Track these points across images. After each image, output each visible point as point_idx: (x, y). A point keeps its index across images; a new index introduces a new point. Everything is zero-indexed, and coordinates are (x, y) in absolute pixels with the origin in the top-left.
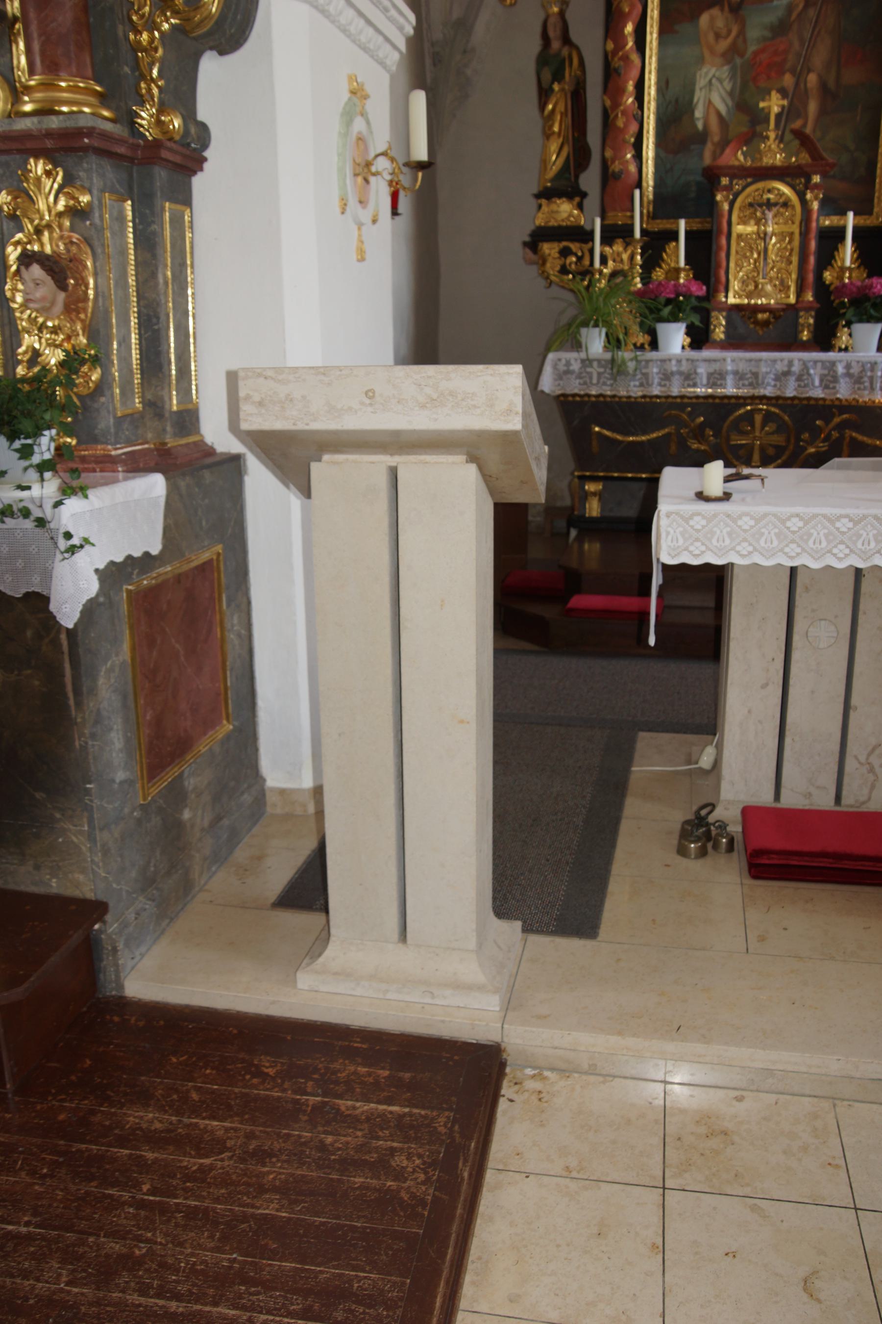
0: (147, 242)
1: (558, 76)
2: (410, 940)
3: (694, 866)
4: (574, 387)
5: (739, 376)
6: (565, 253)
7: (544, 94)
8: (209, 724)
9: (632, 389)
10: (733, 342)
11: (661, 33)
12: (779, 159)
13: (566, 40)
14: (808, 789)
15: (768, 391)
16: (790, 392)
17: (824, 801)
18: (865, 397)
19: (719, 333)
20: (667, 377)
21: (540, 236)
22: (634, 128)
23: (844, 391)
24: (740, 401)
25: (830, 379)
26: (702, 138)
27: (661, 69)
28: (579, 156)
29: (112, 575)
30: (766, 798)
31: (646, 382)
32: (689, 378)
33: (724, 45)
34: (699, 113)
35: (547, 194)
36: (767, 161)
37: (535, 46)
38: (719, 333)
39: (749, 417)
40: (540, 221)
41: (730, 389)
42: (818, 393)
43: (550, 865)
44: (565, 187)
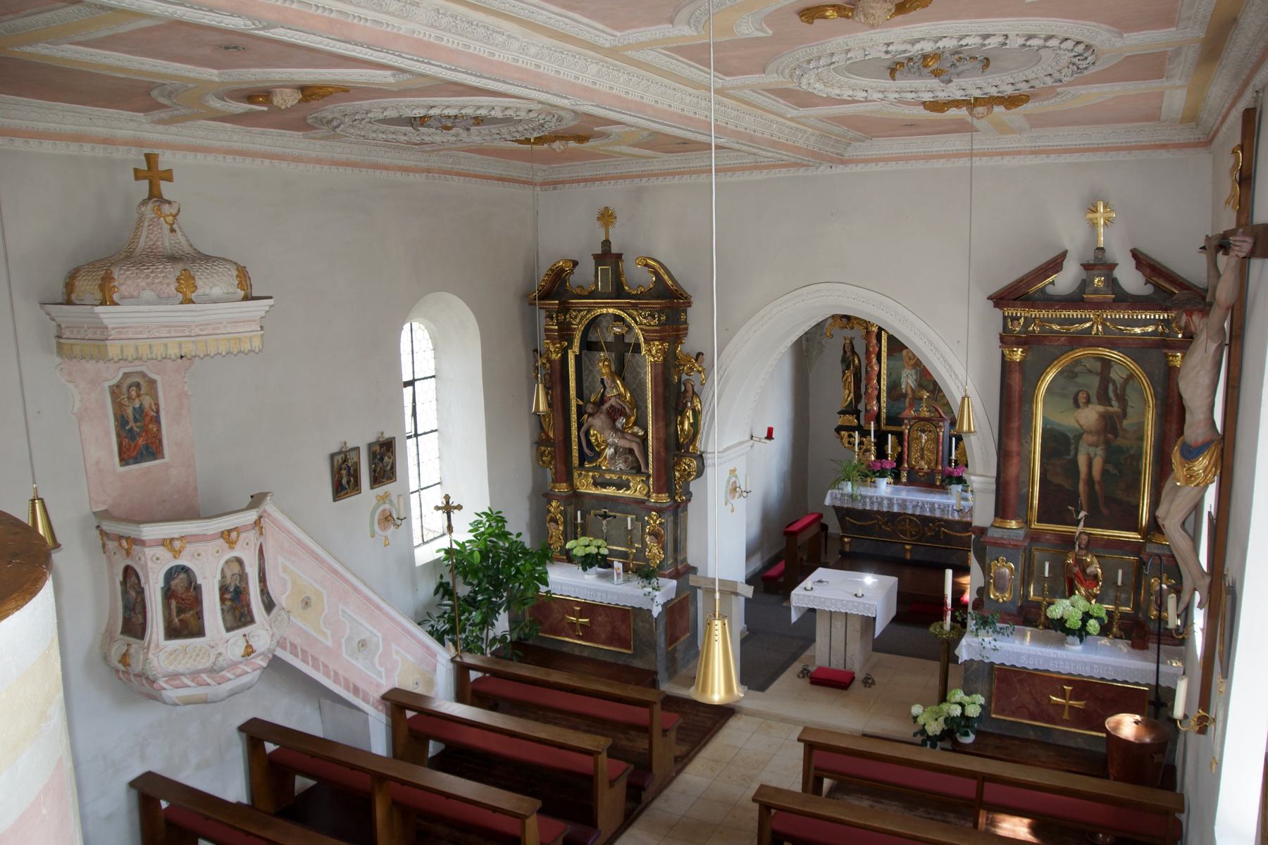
0: (676, 523)
1: (848, 368)
2: (719, 681)
3: (800, 681)
4: (838, 504)
5: (899, 505)
6: (850, 436)
7: (844, 373)
8: (683, 634)
9: (860, 506)
10: (912, 482)
11: (889, 355)
12: (927, 414)
13: (854, 353)
14: (837, 664)
15: (910, 512)
16: (918, 513)
17: (841, 667)
18: (945, 517)
19: (904, 480)
20: (872, 503)
21: (839, 429)
22: (876, 393)
23: (938, 514)
24: (898, 514)
25: (932, 509)
26: (905, 396)
27: (888, 369)
28: (858, 397)
29: (664, 605)
30: (826, 665)
31: (864, 504)
32: (880, 504)
33: (912, 362)
34: (903, 386)
35: (842, 413)
36: (922, 415)
37: (841, 352)
38: (904, 480)
39: (904, 520)
40: (841, 421)
41: (896, 509)
42: (928, 514)
43: (755, 673)
44: (852, 410)
